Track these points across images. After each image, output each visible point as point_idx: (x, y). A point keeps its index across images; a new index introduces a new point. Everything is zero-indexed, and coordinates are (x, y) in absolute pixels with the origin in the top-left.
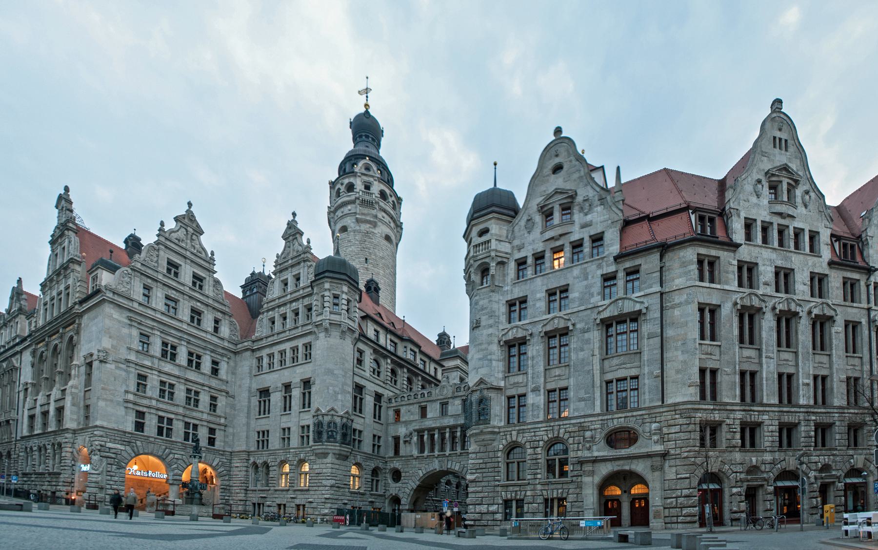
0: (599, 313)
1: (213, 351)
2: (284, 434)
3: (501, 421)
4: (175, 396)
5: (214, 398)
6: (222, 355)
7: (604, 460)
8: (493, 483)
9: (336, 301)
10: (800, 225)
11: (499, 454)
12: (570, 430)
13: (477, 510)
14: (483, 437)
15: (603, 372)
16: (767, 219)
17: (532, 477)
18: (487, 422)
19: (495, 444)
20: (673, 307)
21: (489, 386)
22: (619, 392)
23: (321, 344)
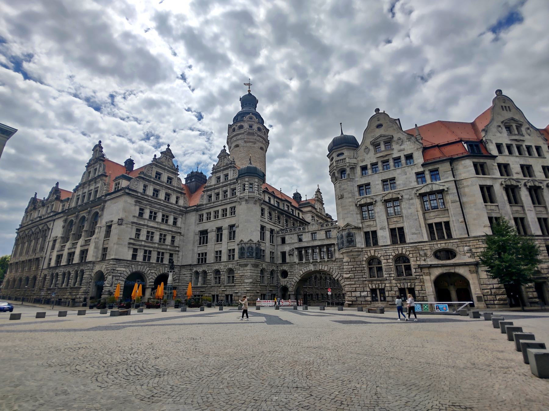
0: (417, 190)
1: (175, 213)
2: (217, 254)
3: (362, 245)
6: (179, 214)
7: (437, 266)
8: (362, 279)
9: (251, 186)
10: (529, 144)
11: (364, 263)
12: (410, 250)
13: (353, 295)
14: (352, 254)
15: (425, 219)
16: (509, 142)
17: (388, 275)
19: (360, 257)
20: (464, 187)
21: (353, 227)
22: (439, 230)
23: (241, 209)
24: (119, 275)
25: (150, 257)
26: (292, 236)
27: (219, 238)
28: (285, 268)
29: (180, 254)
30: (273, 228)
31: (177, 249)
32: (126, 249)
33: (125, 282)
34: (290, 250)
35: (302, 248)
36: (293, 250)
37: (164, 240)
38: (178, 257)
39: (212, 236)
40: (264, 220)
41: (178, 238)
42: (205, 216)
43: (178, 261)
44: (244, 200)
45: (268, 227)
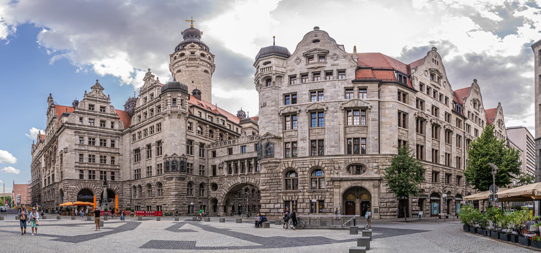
3: (281, 156)
5: (113, 158)
14: (269, 165)
18: (272, 156)
25: (94, 176)
26: (223, 149)
27: (149, 156)
28: (215, 180)
29: (121, 171)
30: (203, 141)
31: (118, 167)
34: (220, 164)
35: (230, 161)
36: (223, 163)
37: (105, 160)
39: (144, 153)
40: (191, 134)
41: (117, 158)
42: (137, 135)
44: (167, 115)
45: (197, 140)
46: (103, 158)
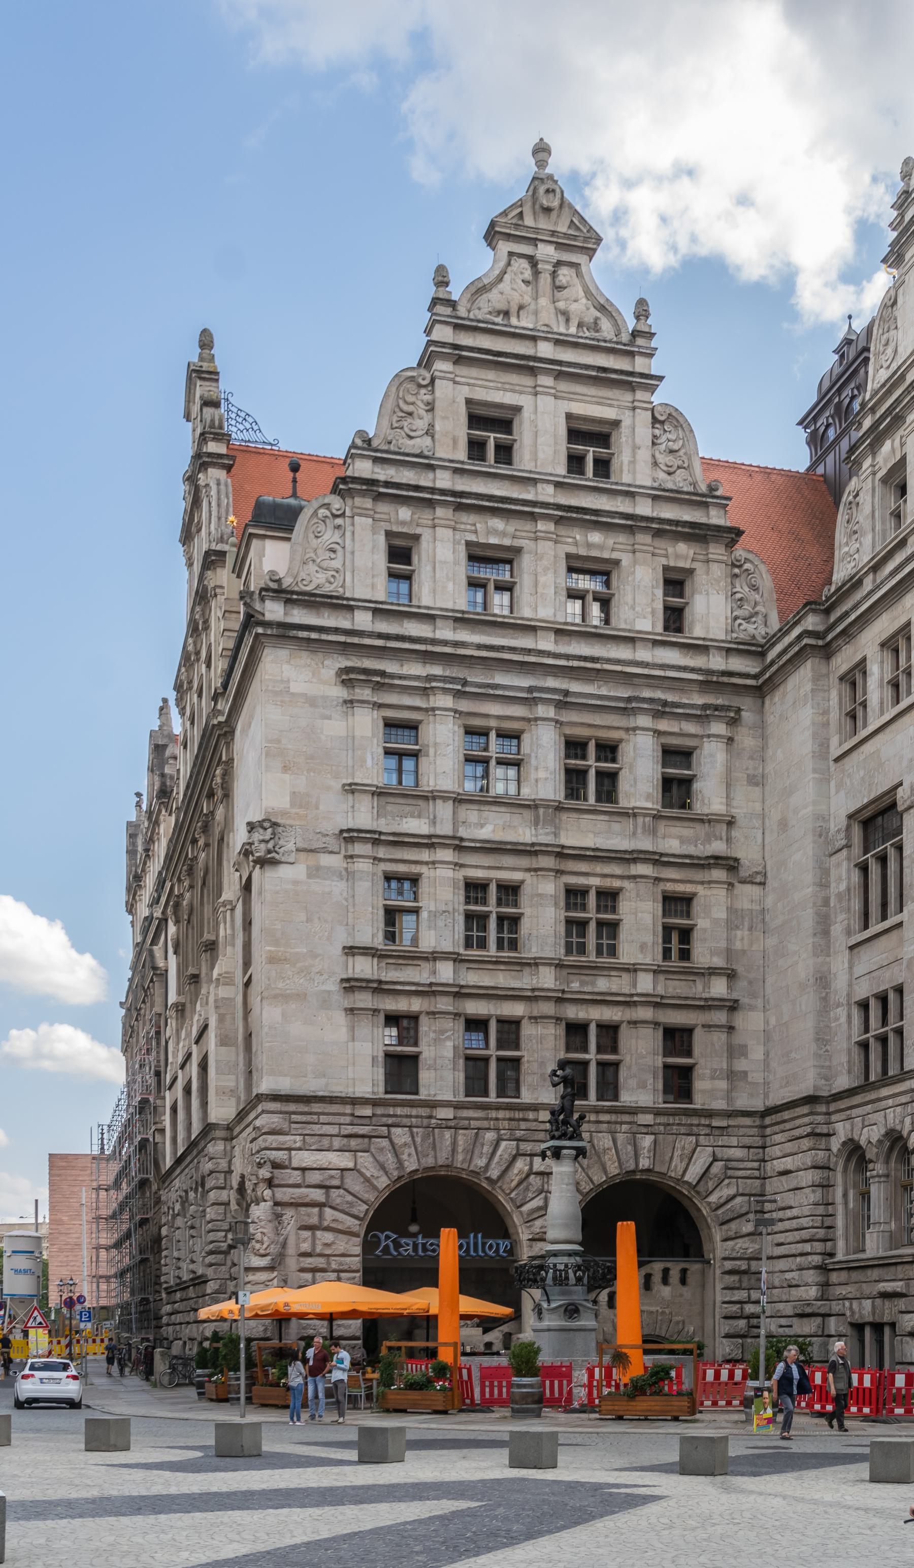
1: (661, 710)
4: (525, 926)
5: (677, 904)
6: (704, 715)
24: (318, 1195)
31: (719, 988)
32: (336, 1027)
33: (369, 1246)
37: (610, 928)
38: (734, 1051)
41: (712, 907)
43: (732, 1076)
46: (591, 913)
